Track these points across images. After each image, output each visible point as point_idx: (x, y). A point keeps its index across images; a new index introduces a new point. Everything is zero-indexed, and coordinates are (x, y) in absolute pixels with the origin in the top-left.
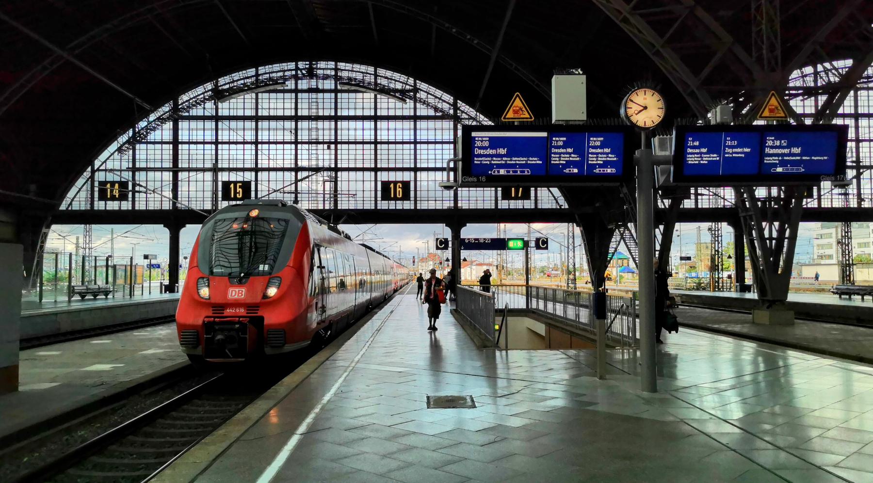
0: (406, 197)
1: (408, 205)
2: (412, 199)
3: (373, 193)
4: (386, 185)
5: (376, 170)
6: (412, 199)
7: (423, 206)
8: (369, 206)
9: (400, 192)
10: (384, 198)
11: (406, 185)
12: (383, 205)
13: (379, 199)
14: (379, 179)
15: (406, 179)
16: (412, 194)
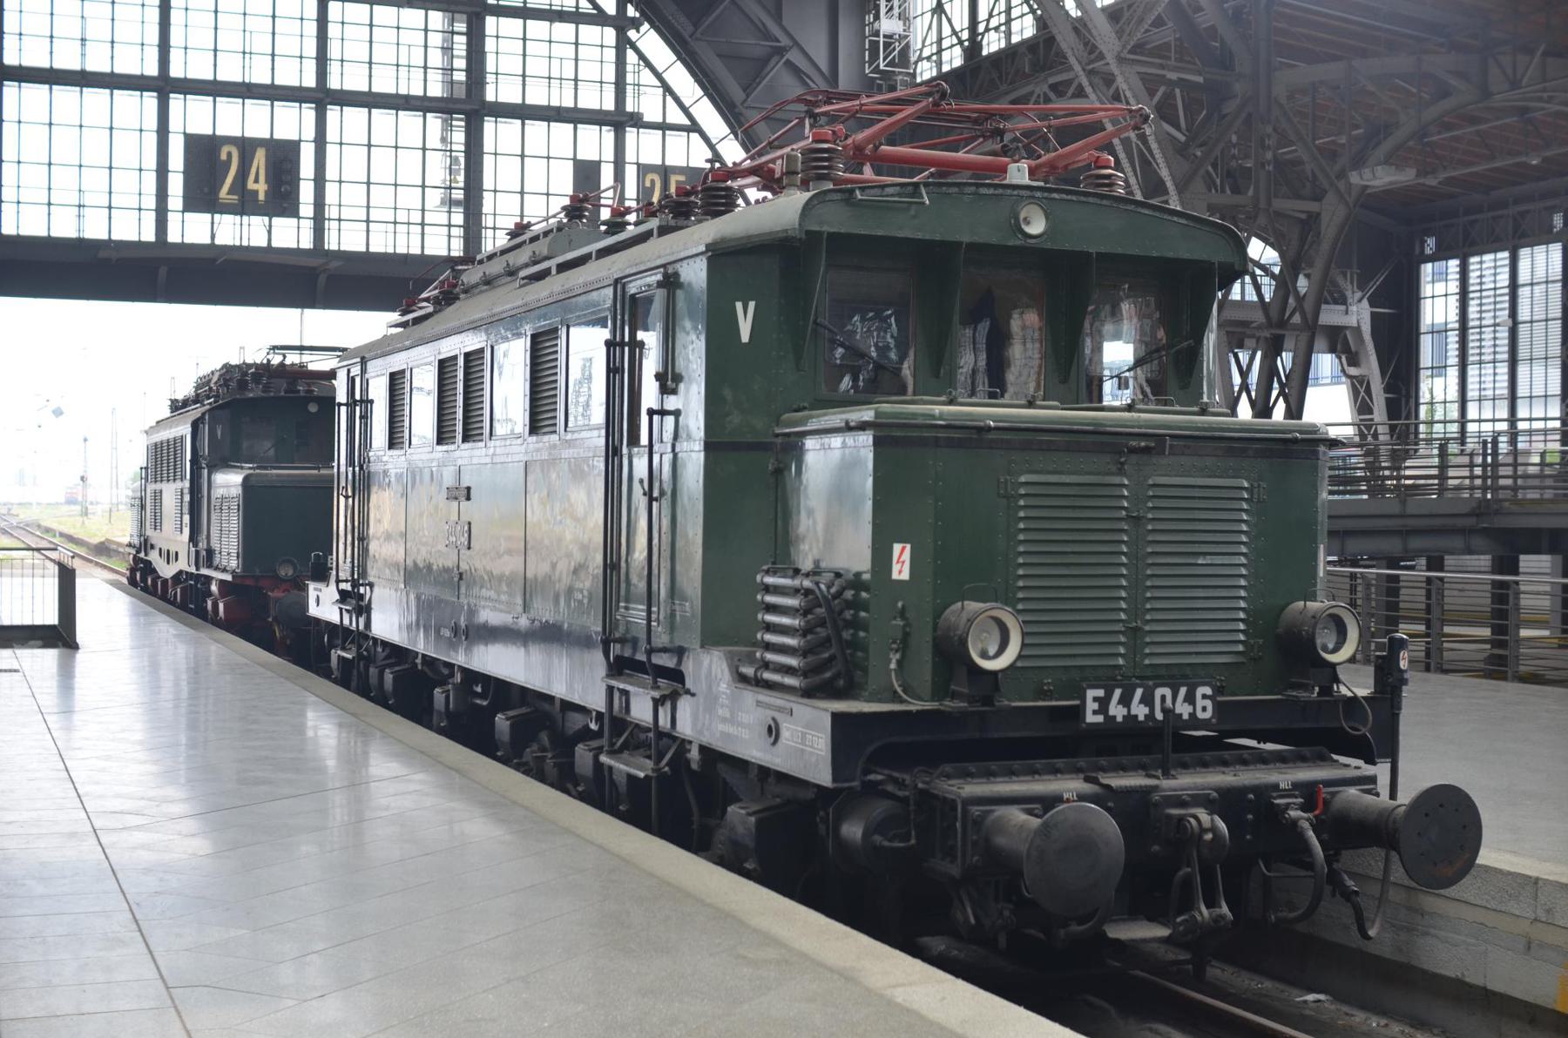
0: (282, 201)
1: (290, 234)
2: (306, 209)
3: (150, 180)
4: (203, 151)
5: (164, 86)
6: (306, 209)
7: (347, 238)
8: (134, 227)
9: (259, 186)
10: (194, 202)
11: (283, 156)
12: (192, 229)
13: (175, 200)
14: (175, 124)
15: (284, 132)
16: (306, 192)
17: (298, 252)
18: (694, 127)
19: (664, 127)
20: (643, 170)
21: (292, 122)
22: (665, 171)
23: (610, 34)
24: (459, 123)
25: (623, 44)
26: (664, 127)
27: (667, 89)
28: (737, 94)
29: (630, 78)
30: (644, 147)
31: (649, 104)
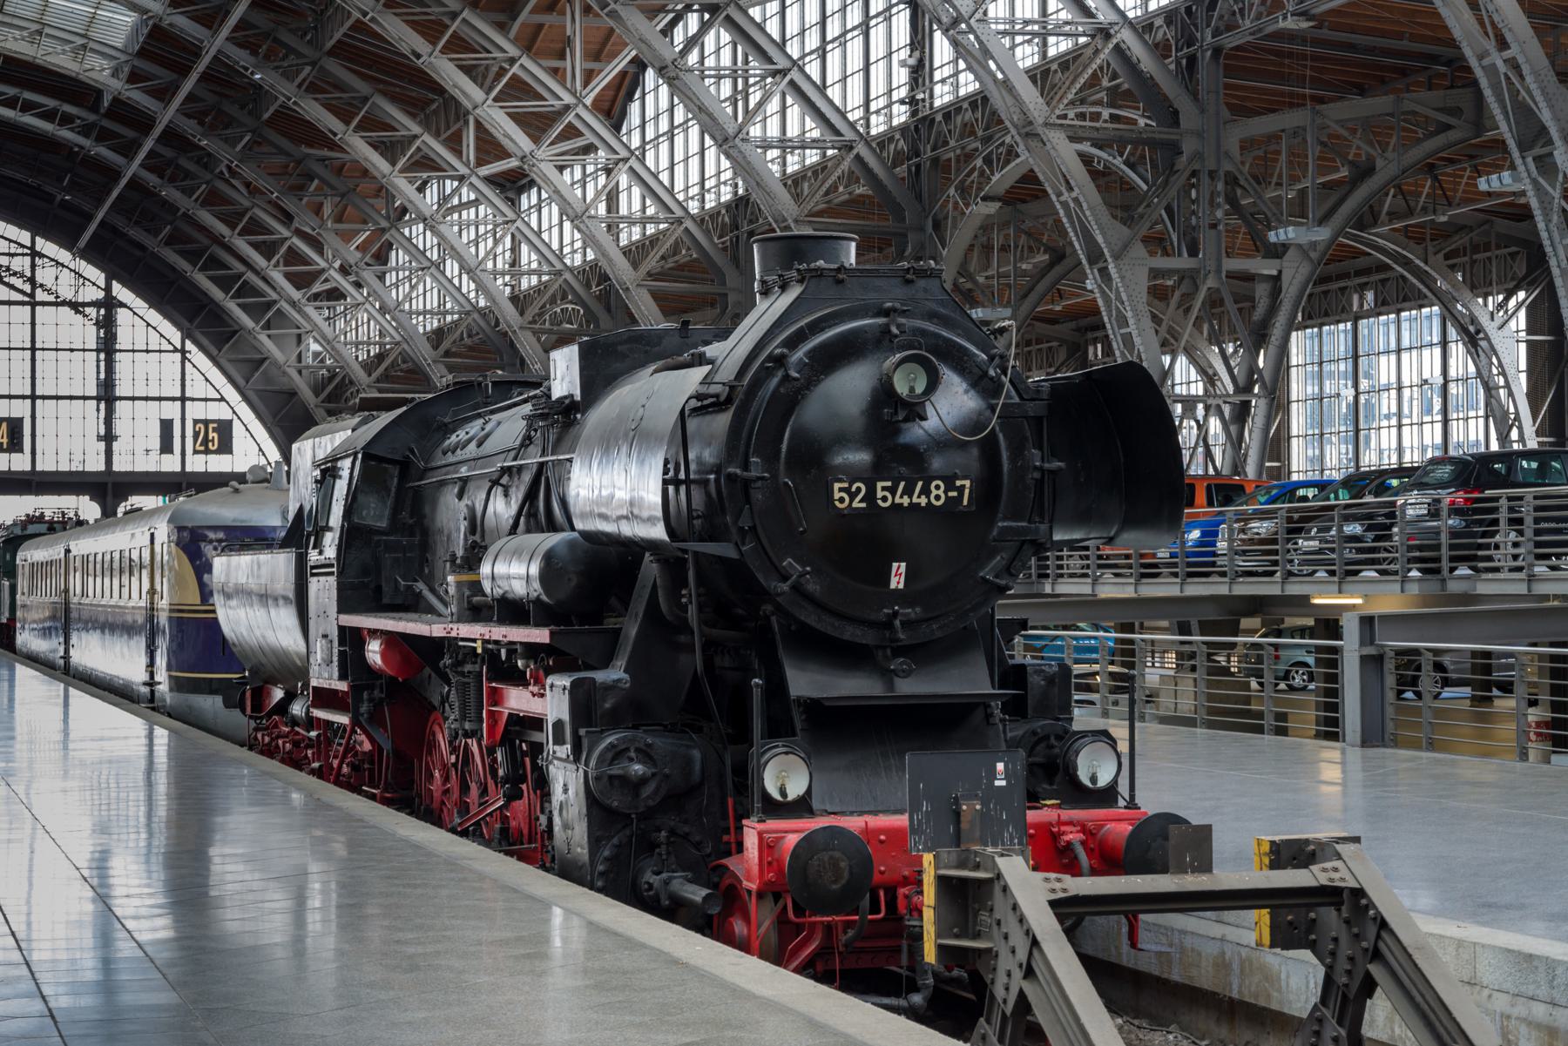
0: (15, 445)
7: (46, 464)
17: (23, 473)
18: (222, 399)
19: (206, 400)
20: (196, 422)
21: (20, 409)
22: (206, 422)
23: (178, 356)
24: (102, 406)
25: (184, 359)
26: (206, 400)
27: (207, 380)
28: (241, 382)
29: (188, 377)
30: (195, 411)
31: (196, 388)
